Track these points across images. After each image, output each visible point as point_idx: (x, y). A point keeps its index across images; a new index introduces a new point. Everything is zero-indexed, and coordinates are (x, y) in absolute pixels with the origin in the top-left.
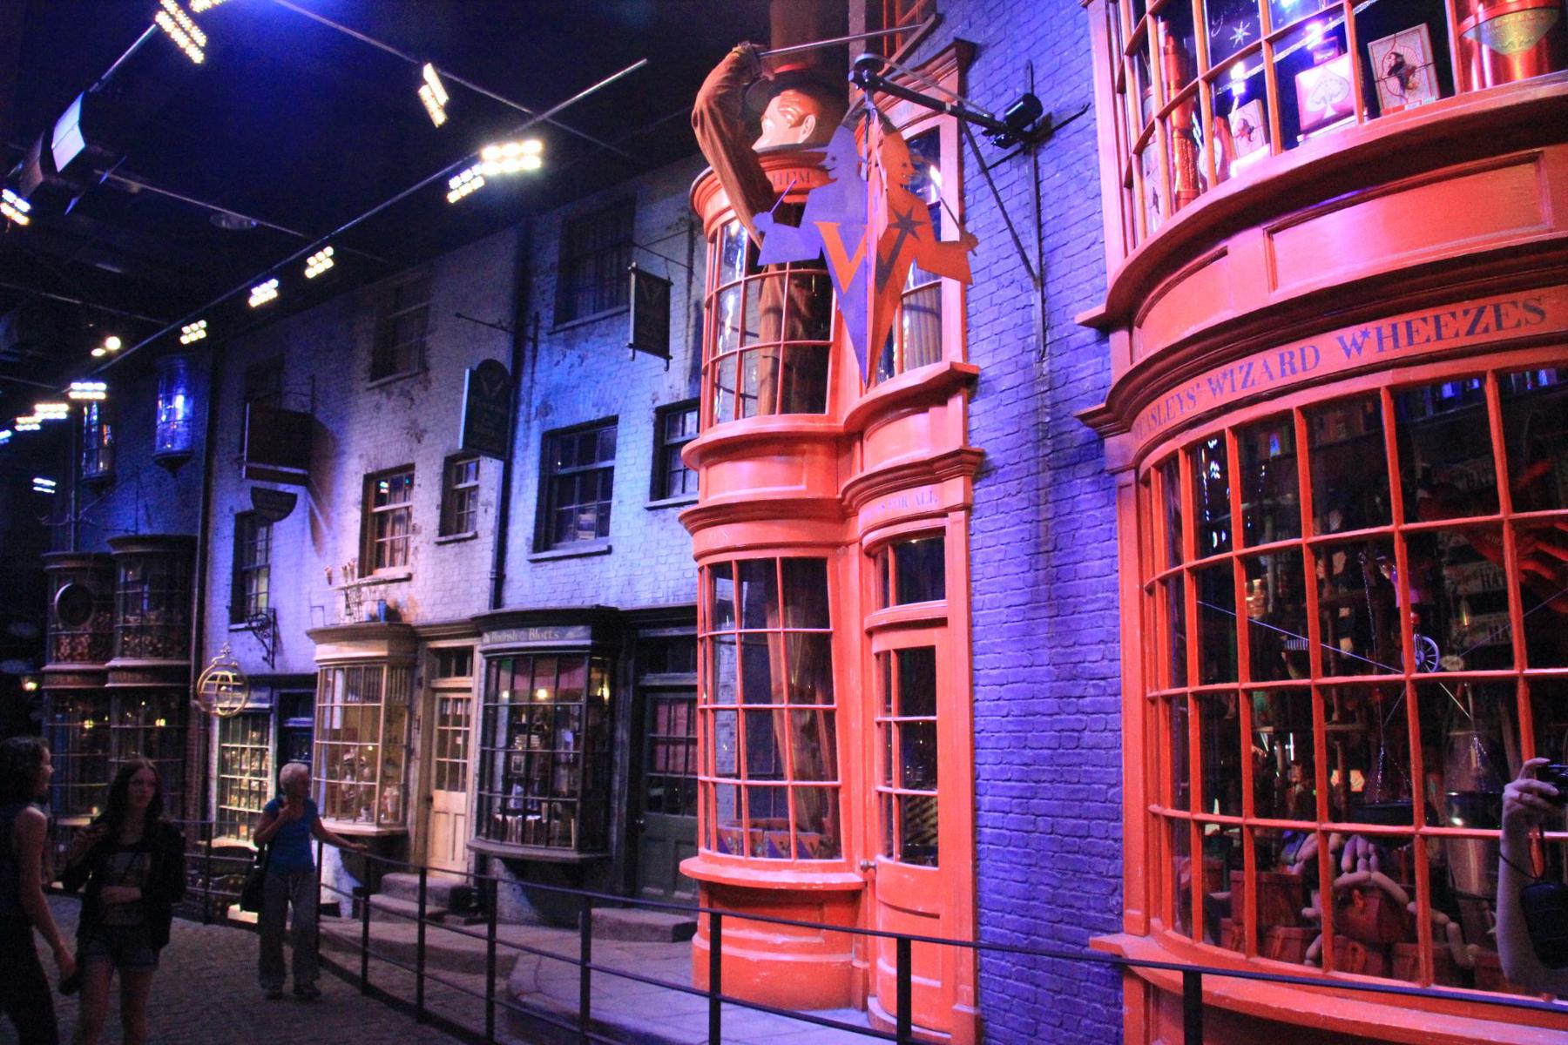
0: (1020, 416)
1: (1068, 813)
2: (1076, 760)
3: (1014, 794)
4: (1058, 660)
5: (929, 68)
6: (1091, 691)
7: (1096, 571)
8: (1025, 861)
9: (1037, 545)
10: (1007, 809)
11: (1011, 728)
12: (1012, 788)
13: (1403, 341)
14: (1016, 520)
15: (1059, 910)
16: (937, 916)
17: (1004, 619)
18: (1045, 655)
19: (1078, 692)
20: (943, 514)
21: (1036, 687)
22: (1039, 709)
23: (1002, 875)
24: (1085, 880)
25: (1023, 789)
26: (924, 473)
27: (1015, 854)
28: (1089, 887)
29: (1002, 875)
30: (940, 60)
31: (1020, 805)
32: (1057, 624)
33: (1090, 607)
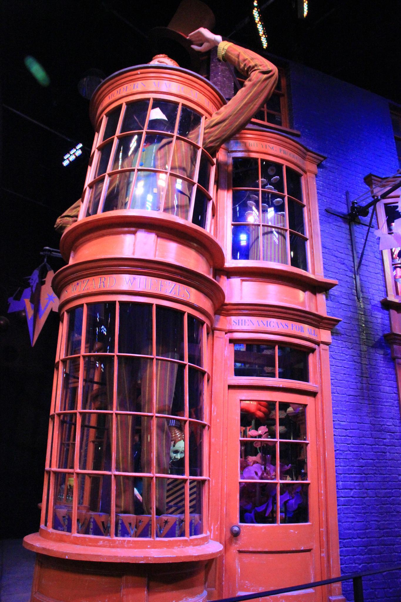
0: (351, 317)
1: (383, 487)
2: (384, 465)
3: (356, 480)
4: (373, 422)
5: (309, 153)
6: (389, 437)
7: (388, 391)
8: (363, 511)
9: (362, 373)
10: (352, 487)
11: (353, 450)
12: (355, 477)
13: (240, 321)
14: (351, 360)
15: (382, 532)
16: (309, 550)
17: (347, 400)
18: (367, 420)
19: (383, 437)
20: (318, 343)
21: (364, 432)
22: (367, 442)
23: (351, 520)
24: (392, 515)
25: (361, 478)
26: (316, 321)
27: (358, 509)
28: (393, 519)
29: (351, 520)
30: (315, 156)
31: (359, 485)
32: (374, 408)
33: (386, 404)
